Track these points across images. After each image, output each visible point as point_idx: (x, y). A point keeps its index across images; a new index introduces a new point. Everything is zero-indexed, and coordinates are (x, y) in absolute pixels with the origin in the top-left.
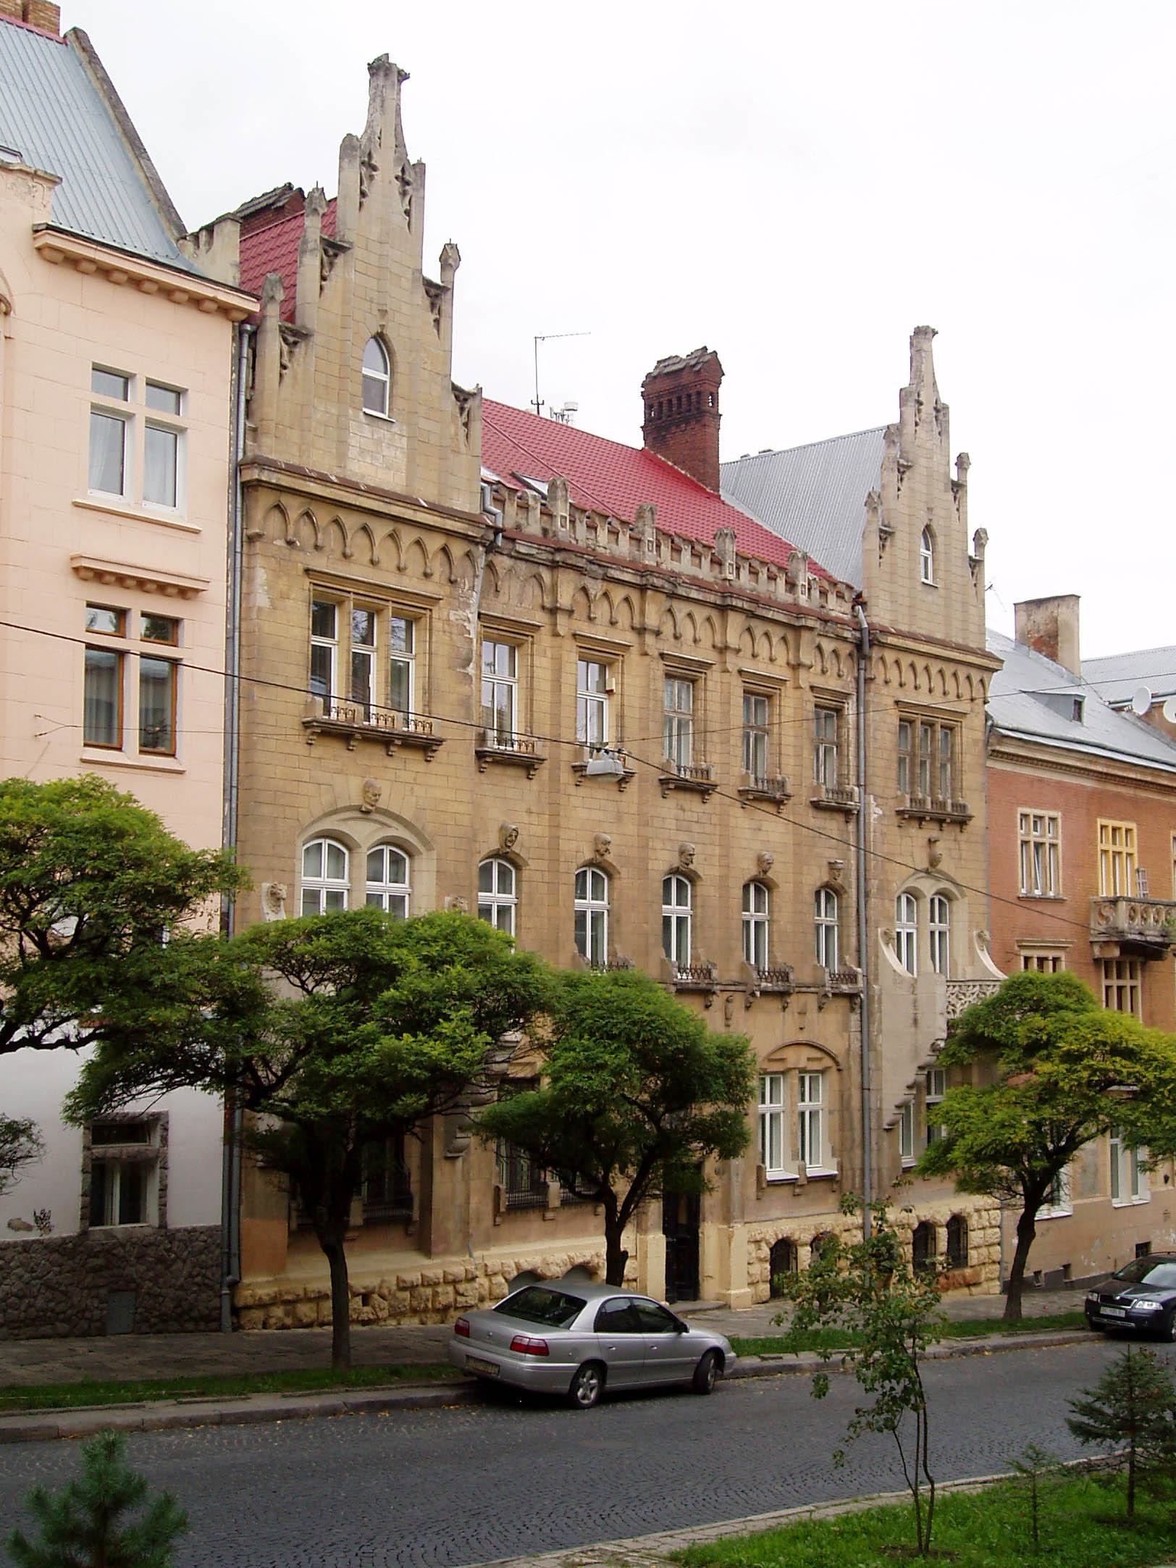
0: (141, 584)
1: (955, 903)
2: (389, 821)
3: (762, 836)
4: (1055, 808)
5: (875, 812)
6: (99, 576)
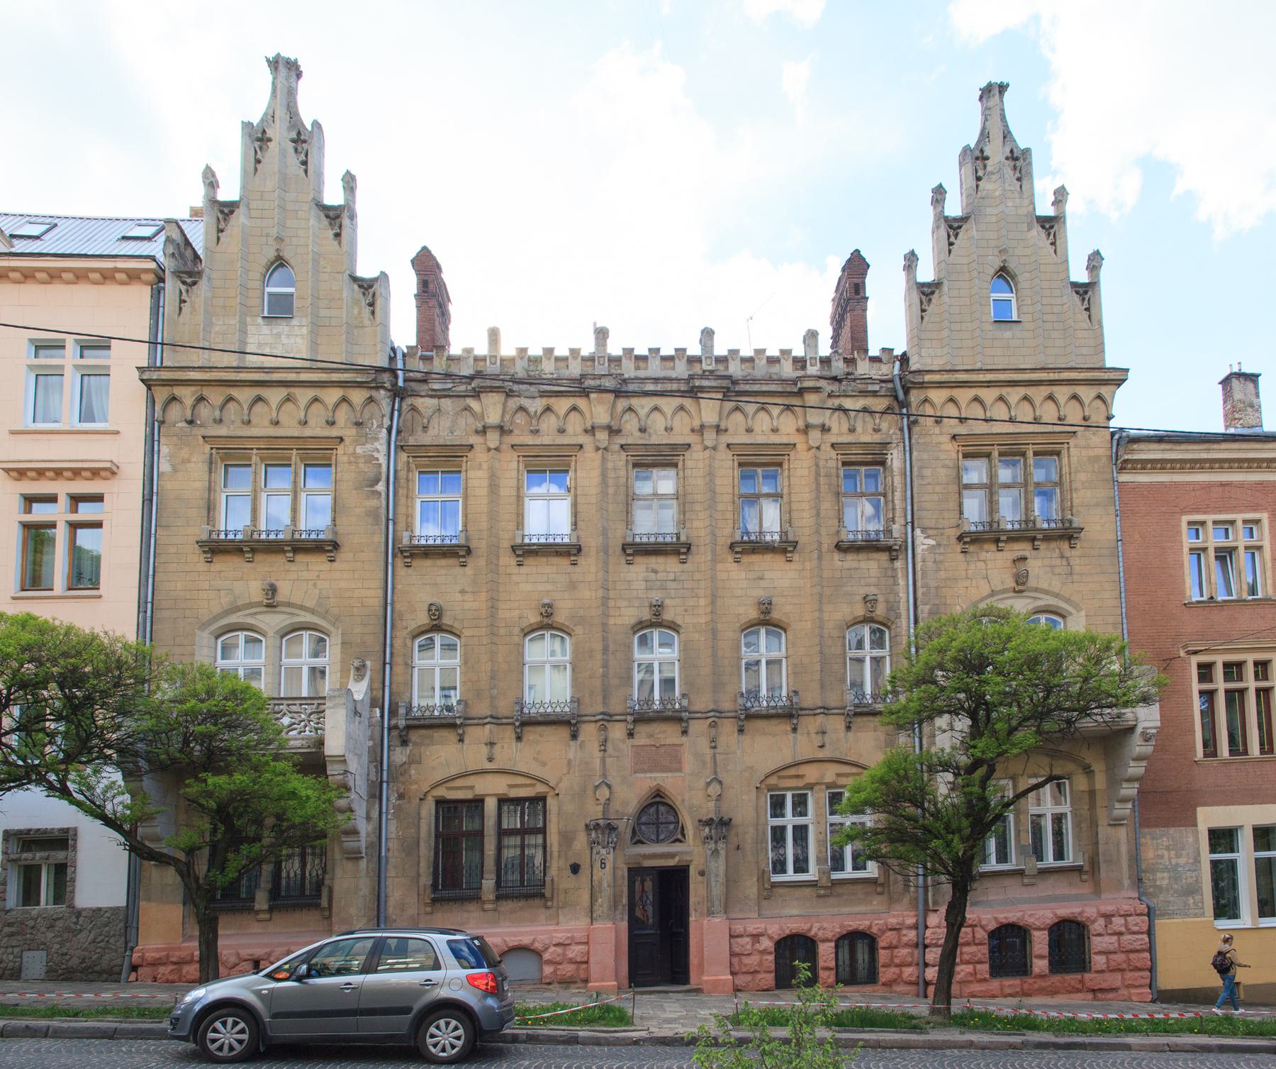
0: (58, 473)
1: (1069, 619)
2: (297, 611)
3: (763, 584)
4: (1255, 508)
5: (923, 543)
6: (21, 474)
